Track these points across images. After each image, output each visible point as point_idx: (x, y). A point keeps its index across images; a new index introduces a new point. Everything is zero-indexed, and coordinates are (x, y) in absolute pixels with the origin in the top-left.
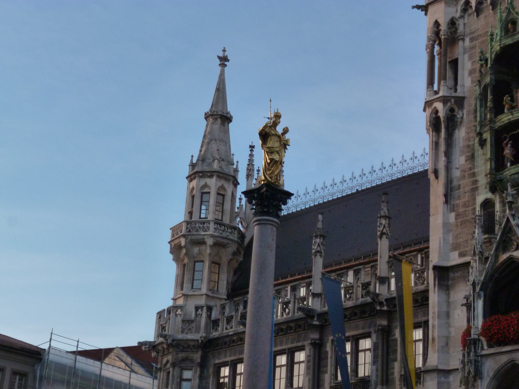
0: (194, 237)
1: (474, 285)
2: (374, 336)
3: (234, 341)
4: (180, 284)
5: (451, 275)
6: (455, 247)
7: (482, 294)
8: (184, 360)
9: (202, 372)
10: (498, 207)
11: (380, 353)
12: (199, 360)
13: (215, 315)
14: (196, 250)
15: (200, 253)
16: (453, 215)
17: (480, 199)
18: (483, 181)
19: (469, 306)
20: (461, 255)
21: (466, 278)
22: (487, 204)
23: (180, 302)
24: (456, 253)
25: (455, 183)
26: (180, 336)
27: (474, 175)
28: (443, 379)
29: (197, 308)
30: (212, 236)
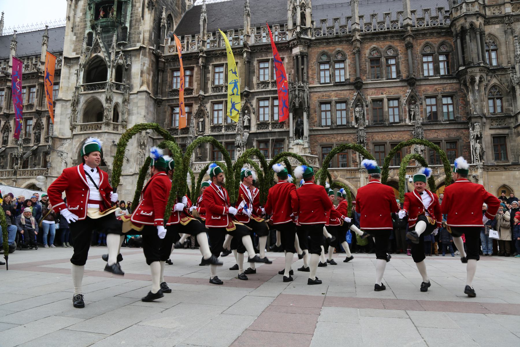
1: (80, 65)
2: (37, 87)
5: (72, 62)
6: (74, 50)
7: (83, 69)
10: (94, 35)
11: (39, 93)
16: (75, 37)
17: (87, 32)
18: (89, 24)
19: (77, 75)
20: (77, 54)
21: (77, 63)
22: (90, 35)
24: (75, 53)
25: (77, 24)
27: (85, 21)
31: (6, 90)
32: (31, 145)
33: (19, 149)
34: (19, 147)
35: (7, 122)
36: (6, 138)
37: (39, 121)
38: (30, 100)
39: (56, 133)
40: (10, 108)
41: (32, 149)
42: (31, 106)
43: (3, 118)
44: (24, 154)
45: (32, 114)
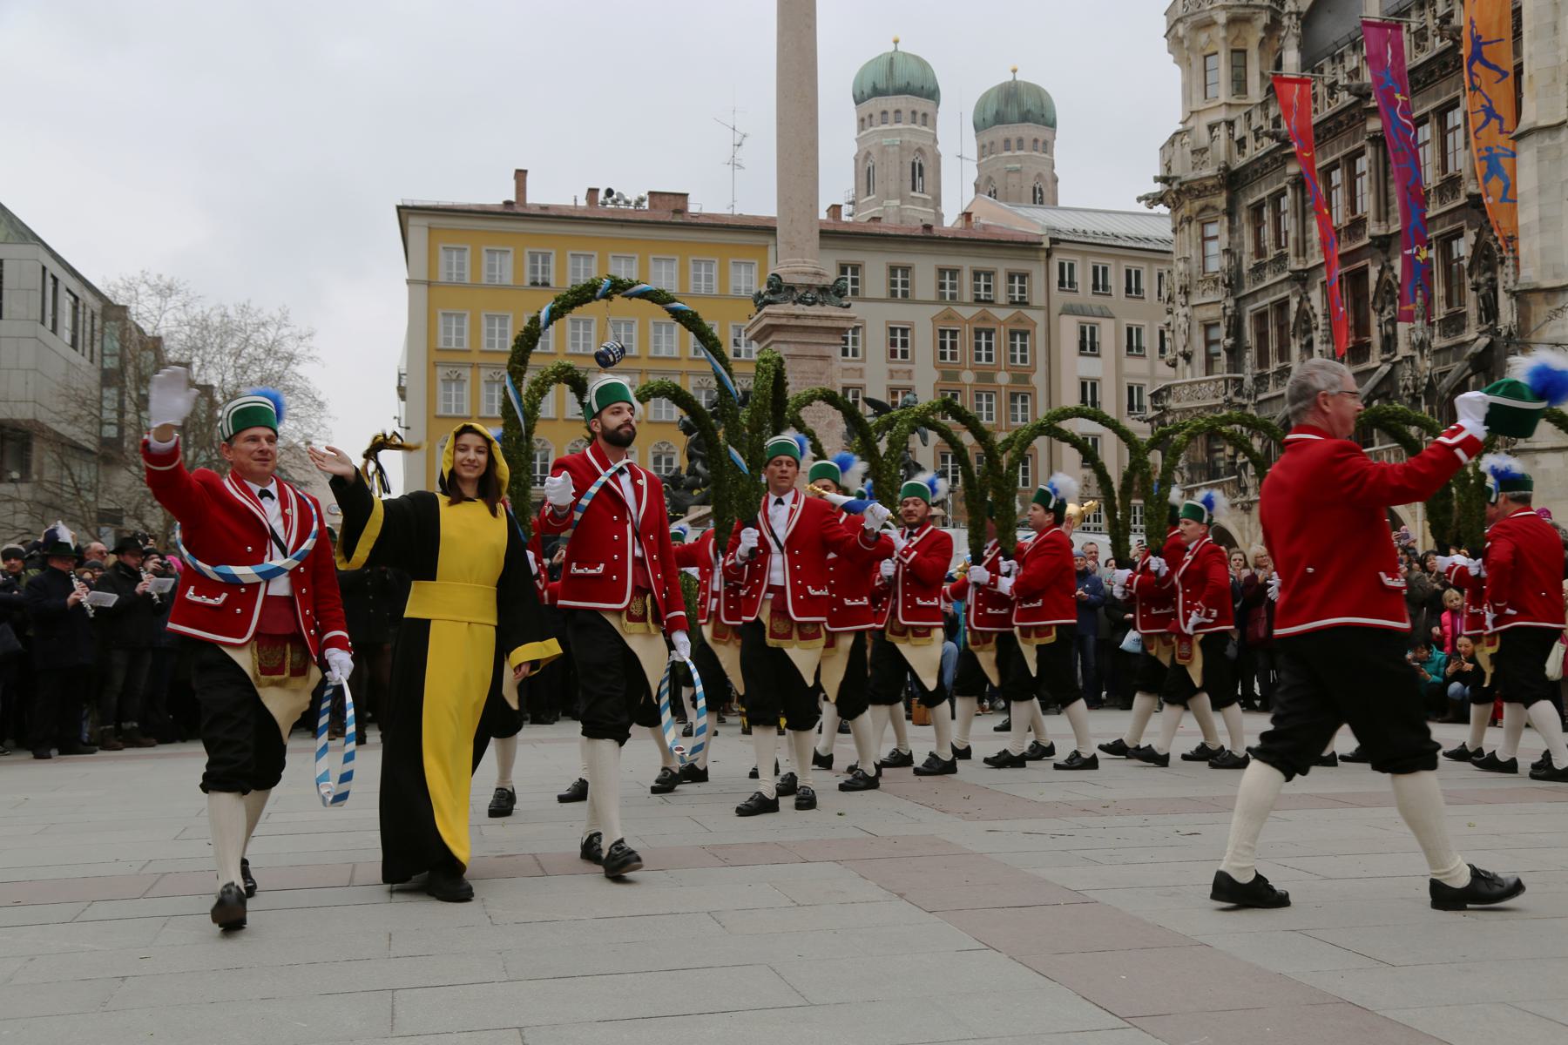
0: (1195, 18)
3: (1266, 166)
4: (1187, 96)
8: (1203, 210)
9: (1231, 222)
12: (1224, 206)
13: (1239, 132)
14: (1203, 37)
15: (1211, 41)
23: (1190, 124)
26: (1191, 176)
28: (1548, 142)
29: (1211, 128)
30: (1224, 7)
31: (1369, 151)
32: (1469, 335)
33: (1418, 360)
34: (1417, 353)
35: (1386, 267)
36: (1390, 328)
37: (1485, 234)
38: (1450, 158)
39: (1531, 274)
40: (1387, 213)
41: (1472, 350)
42: (1451, 184)
43: (1372, 257)
44: (1444, 374)
45: (1458, 214)
